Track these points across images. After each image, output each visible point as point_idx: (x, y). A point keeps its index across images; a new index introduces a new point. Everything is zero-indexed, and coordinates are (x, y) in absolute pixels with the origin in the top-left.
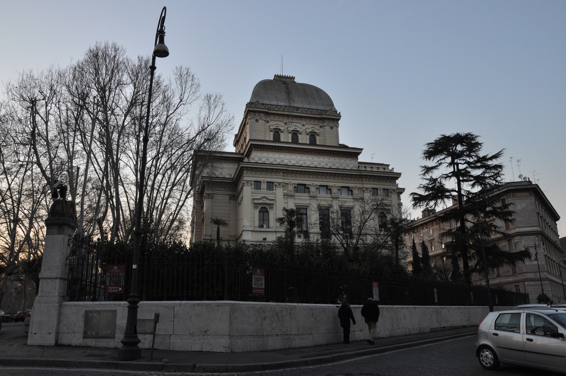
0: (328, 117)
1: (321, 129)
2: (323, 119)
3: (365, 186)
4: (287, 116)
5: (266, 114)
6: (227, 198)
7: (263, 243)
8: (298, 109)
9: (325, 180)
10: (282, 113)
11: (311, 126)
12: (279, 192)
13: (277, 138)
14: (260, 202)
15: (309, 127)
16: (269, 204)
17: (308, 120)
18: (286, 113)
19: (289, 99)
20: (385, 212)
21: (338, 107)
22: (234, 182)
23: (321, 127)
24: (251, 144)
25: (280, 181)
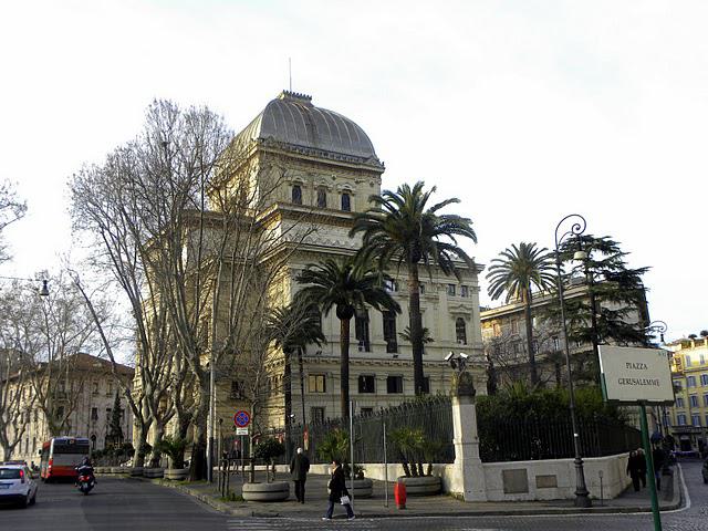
1: (358, 186)
4: (313, 163)
11: (345, 180)
15: (341, 182)
18: (311, 159)
19: (314, 136)
23: (357, 182)
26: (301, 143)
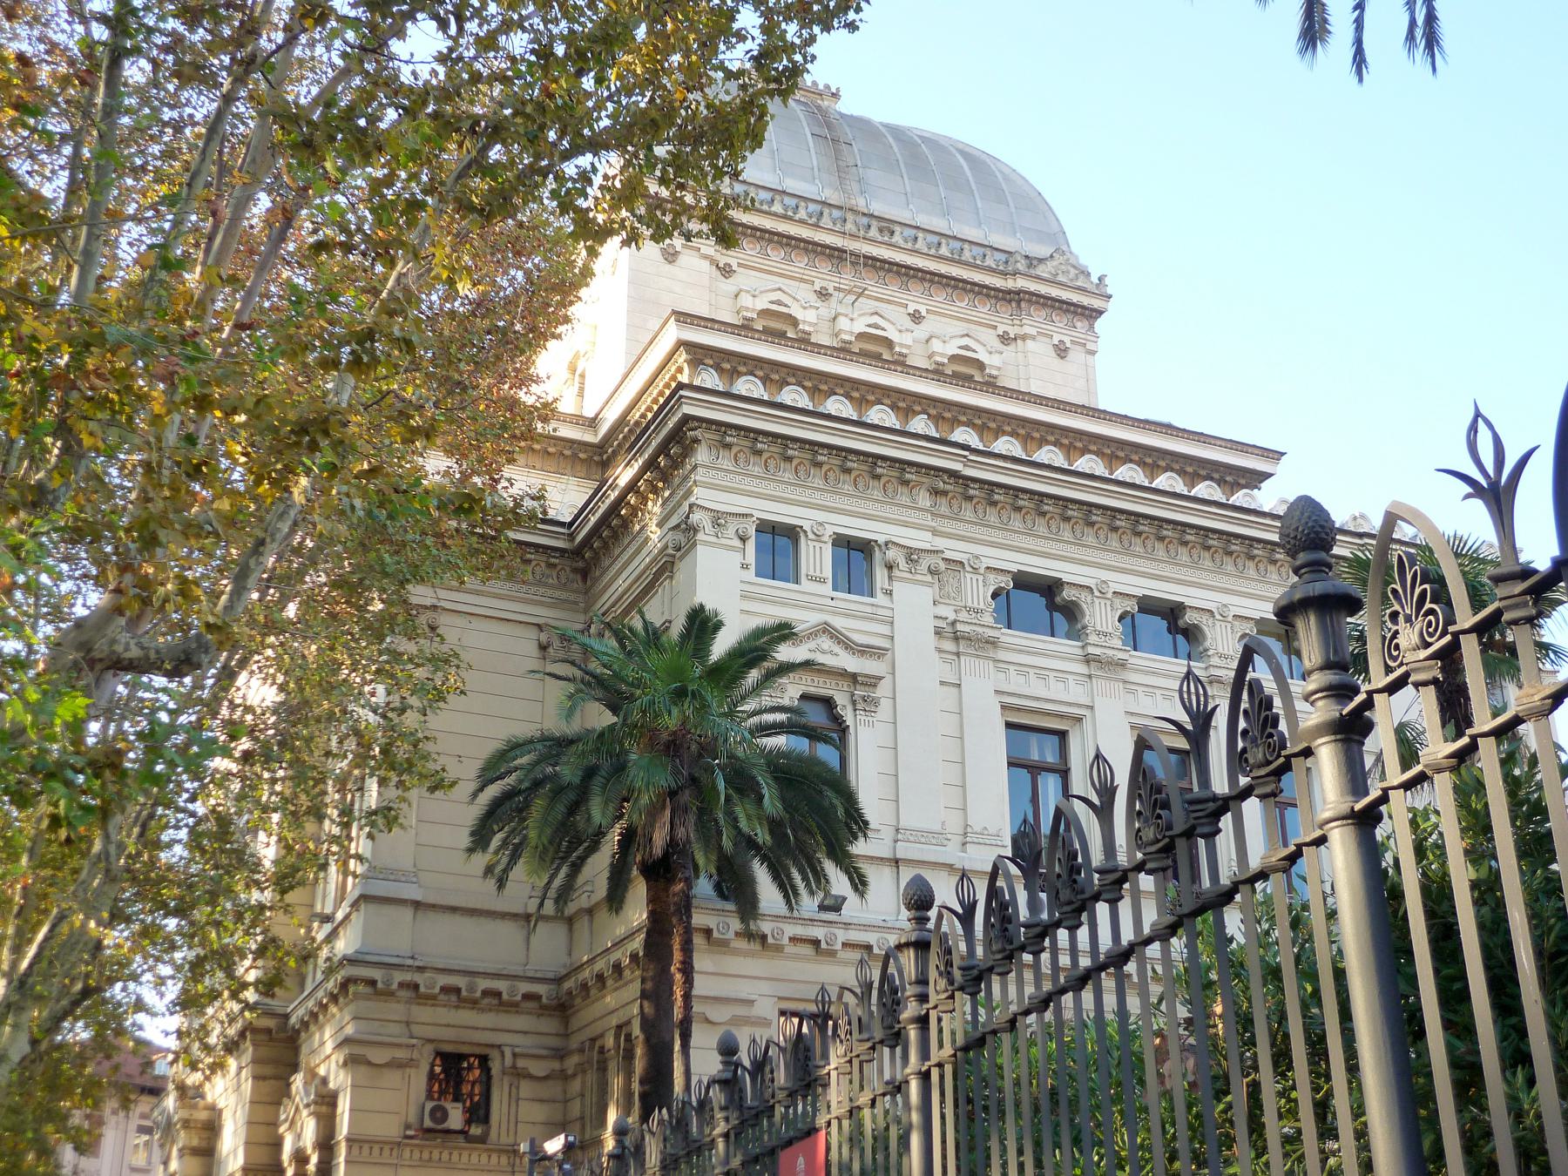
0: (1044, 289)
4: (836, 255)
6: (526, 644)
7: (818, 932)
8: (888, 226)
9: (1168, 571)
11: (961, 327)
12: (911, 608)
16: (853, 678)
17: (940, 296)
21: (1093, 245)
22: (577, 552)
23: (1005, 339)
26: (792, 185)
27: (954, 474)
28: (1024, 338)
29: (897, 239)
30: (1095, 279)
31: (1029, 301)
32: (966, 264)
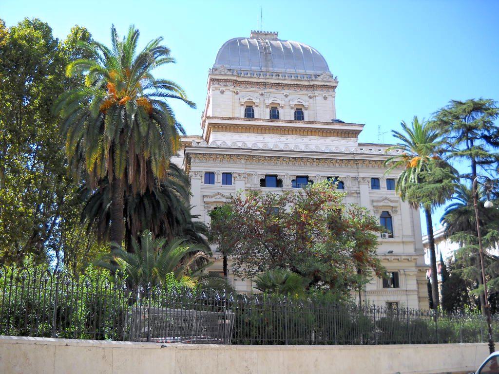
1: (311, 101)
2: (313, 87)
3: (362, 175)
5: (235, 82)
10: (256, 80)
11: (298, 96)
13: (249, 113)
14: (213, 200)
15: (296, 98)
20: (390, 211)
21: (334, 69)
24: (210, 124)
25: (242, 171)
27: (249, 155)
28: (315, 96)
29: (280, 77)
30: (334, 78)
31: (316, 87)
32: (299, 80)
